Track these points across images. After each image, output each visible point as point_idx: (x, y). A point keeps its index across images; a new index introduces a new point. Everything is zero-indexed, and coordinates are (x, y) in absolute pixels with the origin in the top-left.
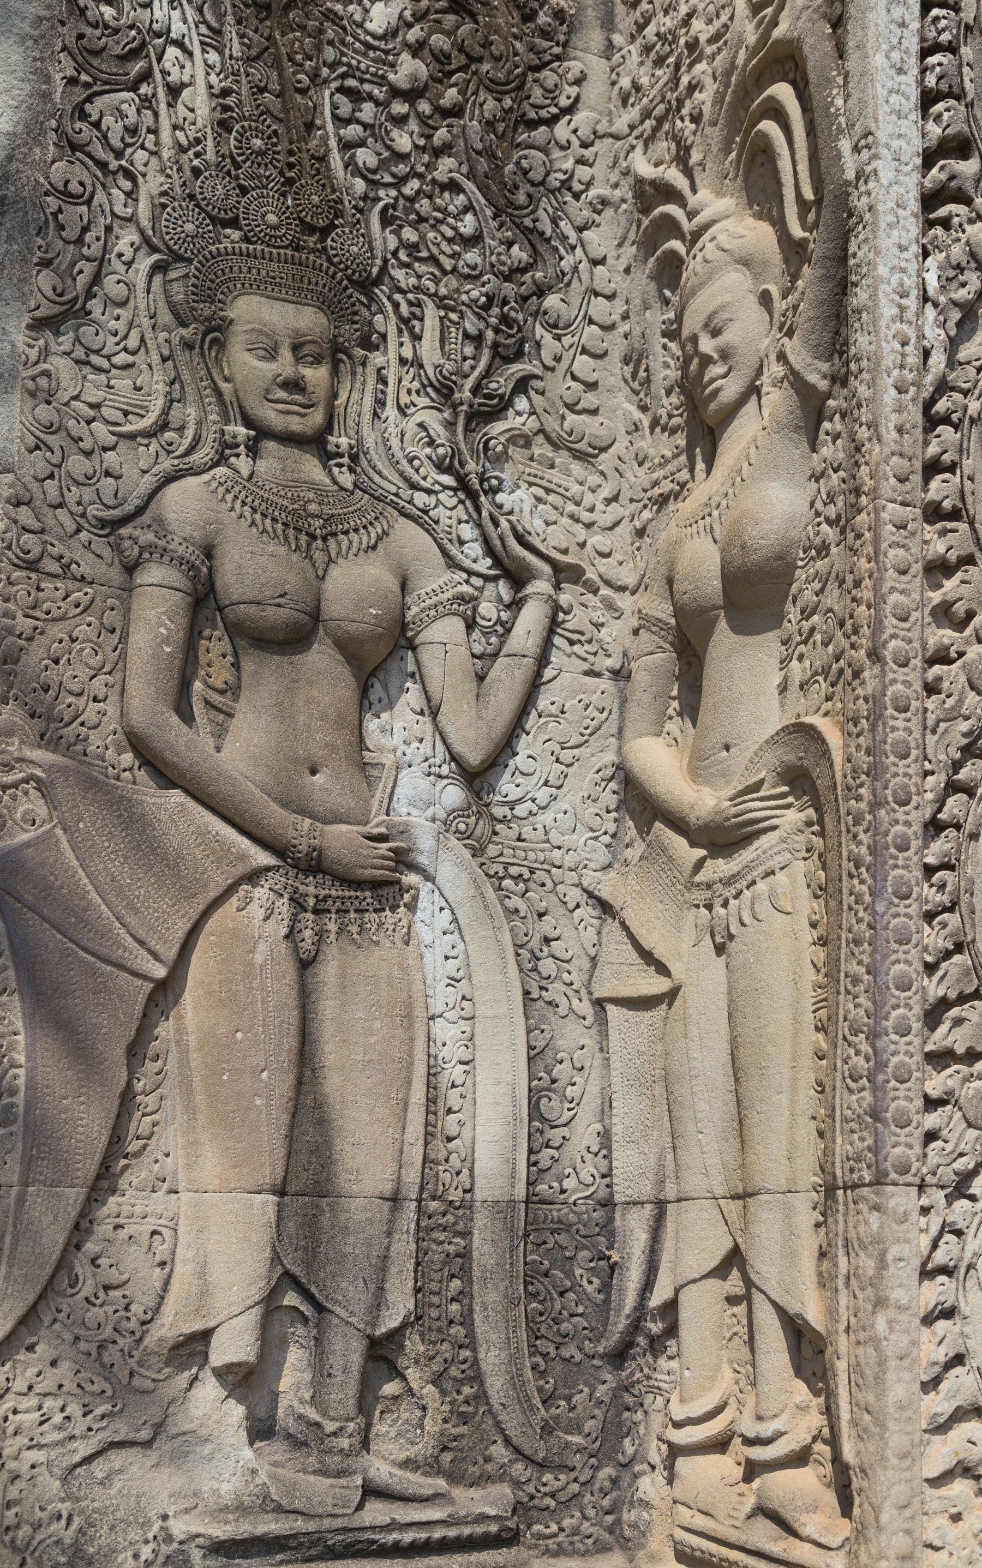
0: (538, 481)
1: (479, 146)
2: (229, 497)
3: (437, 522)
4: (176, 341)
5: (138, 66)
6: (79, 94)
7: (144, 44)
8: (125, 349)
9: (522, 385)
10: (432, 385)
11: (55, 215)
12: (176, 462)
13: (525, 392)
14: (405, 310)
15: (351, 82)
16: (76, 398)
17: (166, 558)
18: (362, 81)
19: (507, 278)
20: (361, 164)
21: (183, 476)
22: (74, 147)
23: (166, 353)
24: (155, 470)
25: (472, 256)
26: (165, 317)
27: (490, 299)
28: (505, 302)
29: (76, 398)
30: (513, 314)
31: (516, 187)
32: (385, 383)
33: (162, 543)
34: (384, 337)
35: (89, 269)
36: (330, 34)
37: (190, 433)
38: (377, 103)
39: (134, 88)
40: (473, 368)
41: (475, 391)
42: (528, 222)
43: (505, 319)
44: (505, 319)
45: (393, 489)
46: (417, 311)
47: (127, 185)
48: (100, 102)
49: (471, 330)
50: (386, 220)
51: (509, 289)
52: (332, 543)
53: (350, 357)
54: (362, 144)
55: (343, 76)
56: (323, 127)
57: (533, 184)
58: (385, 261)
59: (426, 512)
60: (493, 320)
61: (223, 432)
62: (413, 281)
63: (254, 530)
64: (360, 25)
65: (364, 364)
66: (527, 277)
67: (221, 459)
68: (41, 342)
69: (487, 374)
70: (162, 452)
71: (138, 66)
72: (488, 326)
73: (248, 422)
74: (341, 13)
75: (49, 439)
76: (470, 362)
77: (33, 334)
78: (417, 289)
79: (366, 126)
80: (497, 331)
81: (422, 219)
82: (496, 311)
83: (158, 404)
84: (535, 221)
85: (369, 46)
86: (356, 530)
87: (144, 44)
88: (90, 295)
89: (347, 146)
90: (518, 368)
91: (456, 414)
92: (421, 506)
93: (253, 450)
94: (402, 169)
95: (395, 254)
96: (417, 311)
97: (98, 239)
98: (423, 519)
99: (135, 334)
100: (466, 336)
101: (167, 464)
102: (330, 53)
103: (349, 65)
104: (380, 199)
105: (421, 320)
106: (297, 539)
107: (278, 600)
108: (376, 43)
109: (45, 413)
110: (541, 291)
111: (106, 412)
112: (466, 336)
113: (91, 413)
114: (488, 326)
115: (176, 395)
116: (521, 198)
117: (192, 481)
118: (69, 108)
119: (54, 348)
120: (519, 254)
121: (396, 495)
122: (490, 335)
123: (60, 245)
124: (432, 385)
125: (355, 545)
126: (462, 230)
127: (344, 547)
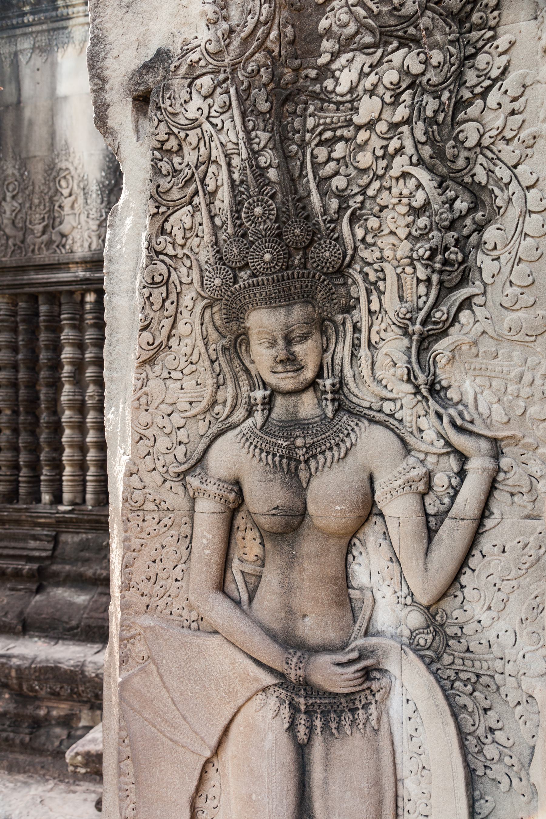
0: (484, 373)
1: (423, 139)
2: (248, 443)
3: (401, 421)
4: (219, 349)
5: (191, 190)
6: (160, 219)
7: (193, 175)
8: (192, 363)
9: (467, 303)
10: (394, 324)
11: (148, 298)
12: (221, 425)
13: (470, 308)
14: (372, 277)
15: (328, 135)
16: (162, 402)
17: (206, 495)
18: (334, 130)
19: (449, 228)
20: (334, 188)
21: (226, 432)
22: (158, 253)
23: (214, 357)
24: (209, 433)
25: (422, 222)
26: (213, 335)
27: (434, 251)
28: (446, 249)
29: (162, 402)
30: (453, 256)
31: (456, 157)
32: (360, 331)
33: (203, 487)
34: (358, 299)
35: (167, 323)
36: (311, 109)
37: (229, 404)
38: (347, 140)
39: (190, 203)
40: (425, 303)
41: (424, 323)
42: (468, 179)
43: (446, 262)
44: (446, 262)
45: (367, 405)
46: (381, 275)
47: (188, 263)
48: (172, 219)
49: (423, 277)
50: (353, 220)
51: (451, 237)
52: (313, 464)
53: (334, 322)
54: (337, 173)
55: (320, 134)
56: (307, 176)
57: (470, 149)
58: (355, 249)
59: (392, 416)
60: (438, 266)
61: (249, 397)
62: (377, 254)
63: (261, 464)
64: (334, 91)
65: (344, 324)
66: (468, 221)
67: (250, 413)
68: (144, 375)
69: (436, 305)
70: (212, 420)
71: (191, 190)
72: (433, 271)
73: (265, 386)
74: (318, 90)
75: (147, 433)
76: (424, 299)
77: (140, 371)
78: (382, 259)
79: (338, 160)
80: (441, 272)
81: (383, 208)
82: (439, 257)
83: (208, 392)
84: (472, 176)
85: (338, 104)
86: (331, 449)
87: (193, 175)
88: (169, 337)
89: (322, 182)
90: (462, 294)
91: (411, 341)
92: (388, 412)
93: (268, 403)
94: (365, 180)
95: (363, 240)
96: (381, 275)
97: (172, 303)
98: (389, 423)
99: (196, 352)
100: (419, 281)
101: (214, 429)
102: (310, 123)
103: (325, 123)
104: (349, 207)
105: (385, 279)
106: (289, 465)
107: (274, 512)
108: (344, 99)
109: (144, 417)
110: (480, 228)
111: (179, 406)
112: (419, 281)
113: (170, 409)
114: (433, 271)
115: (221, 382)
116: (461, 163)
117: (230, 434)
118: (155, 231)
119: (151, 375)
120: (461, 206)
121: (370, 408)
122: (435, 278)
123: (152, 314)
124: (394, 324)
125: (329, 460)
126: (414, 204)
127: (321, 464)
